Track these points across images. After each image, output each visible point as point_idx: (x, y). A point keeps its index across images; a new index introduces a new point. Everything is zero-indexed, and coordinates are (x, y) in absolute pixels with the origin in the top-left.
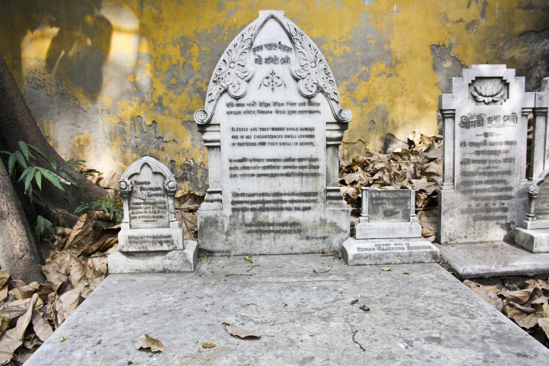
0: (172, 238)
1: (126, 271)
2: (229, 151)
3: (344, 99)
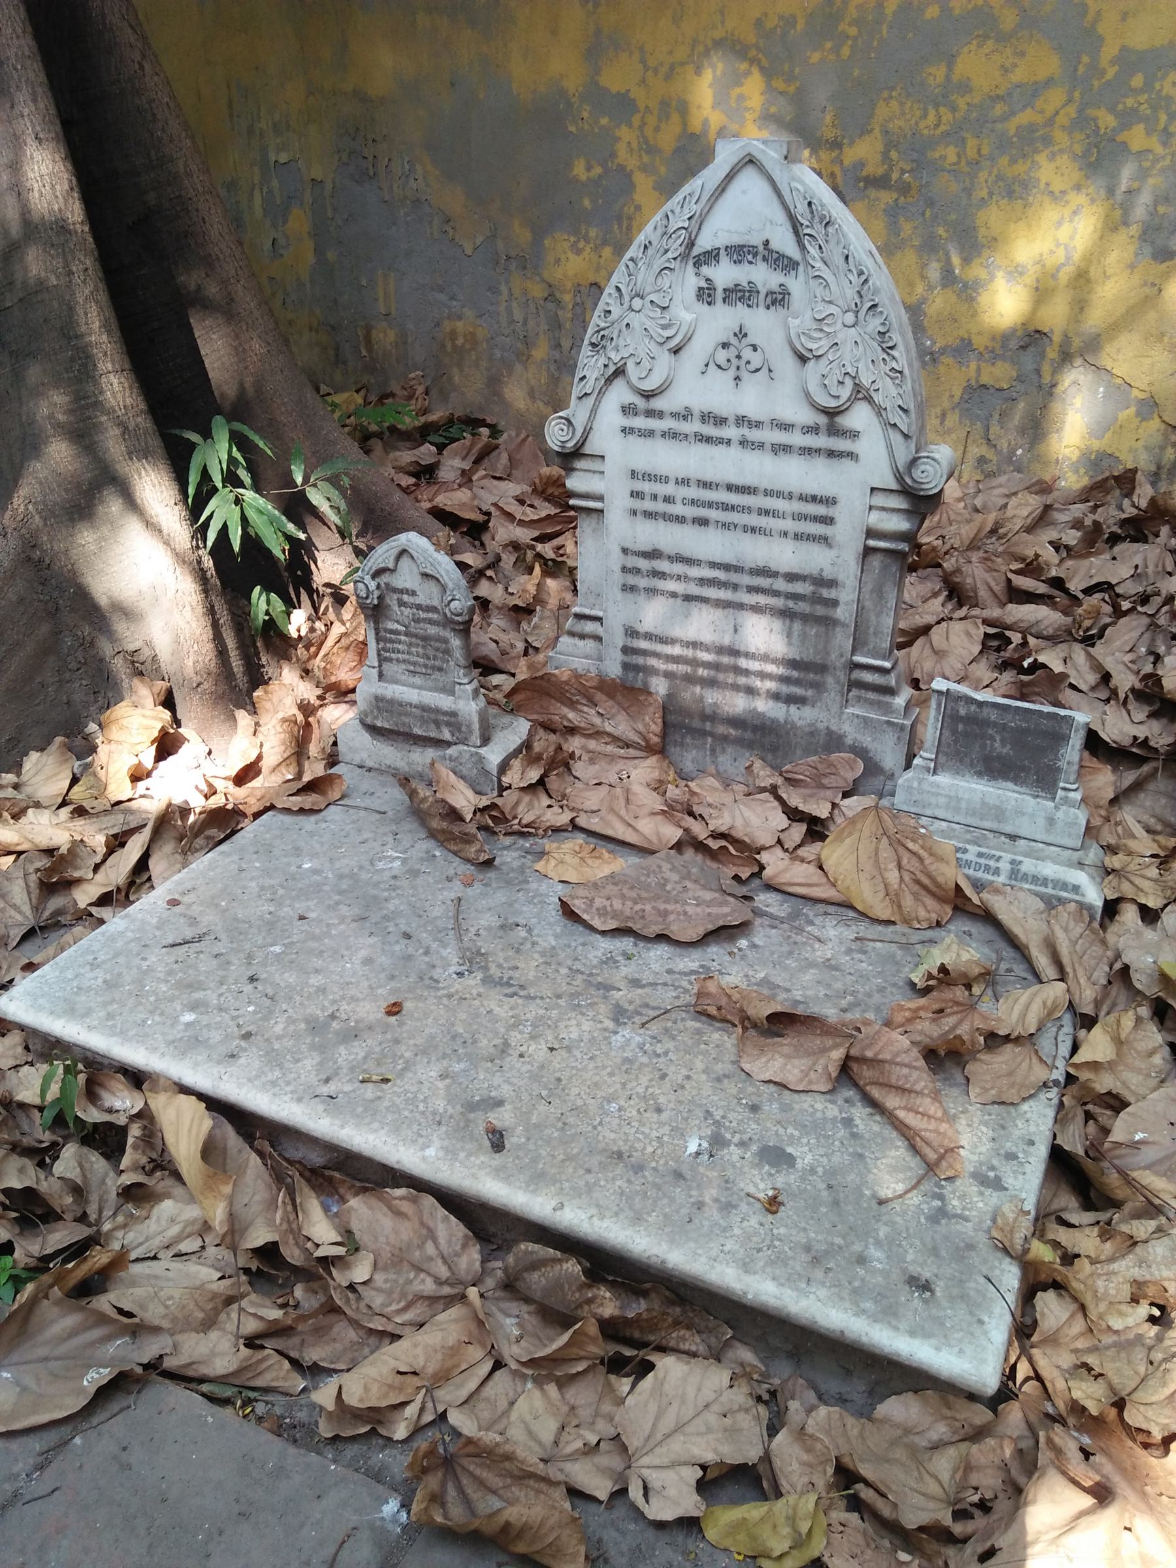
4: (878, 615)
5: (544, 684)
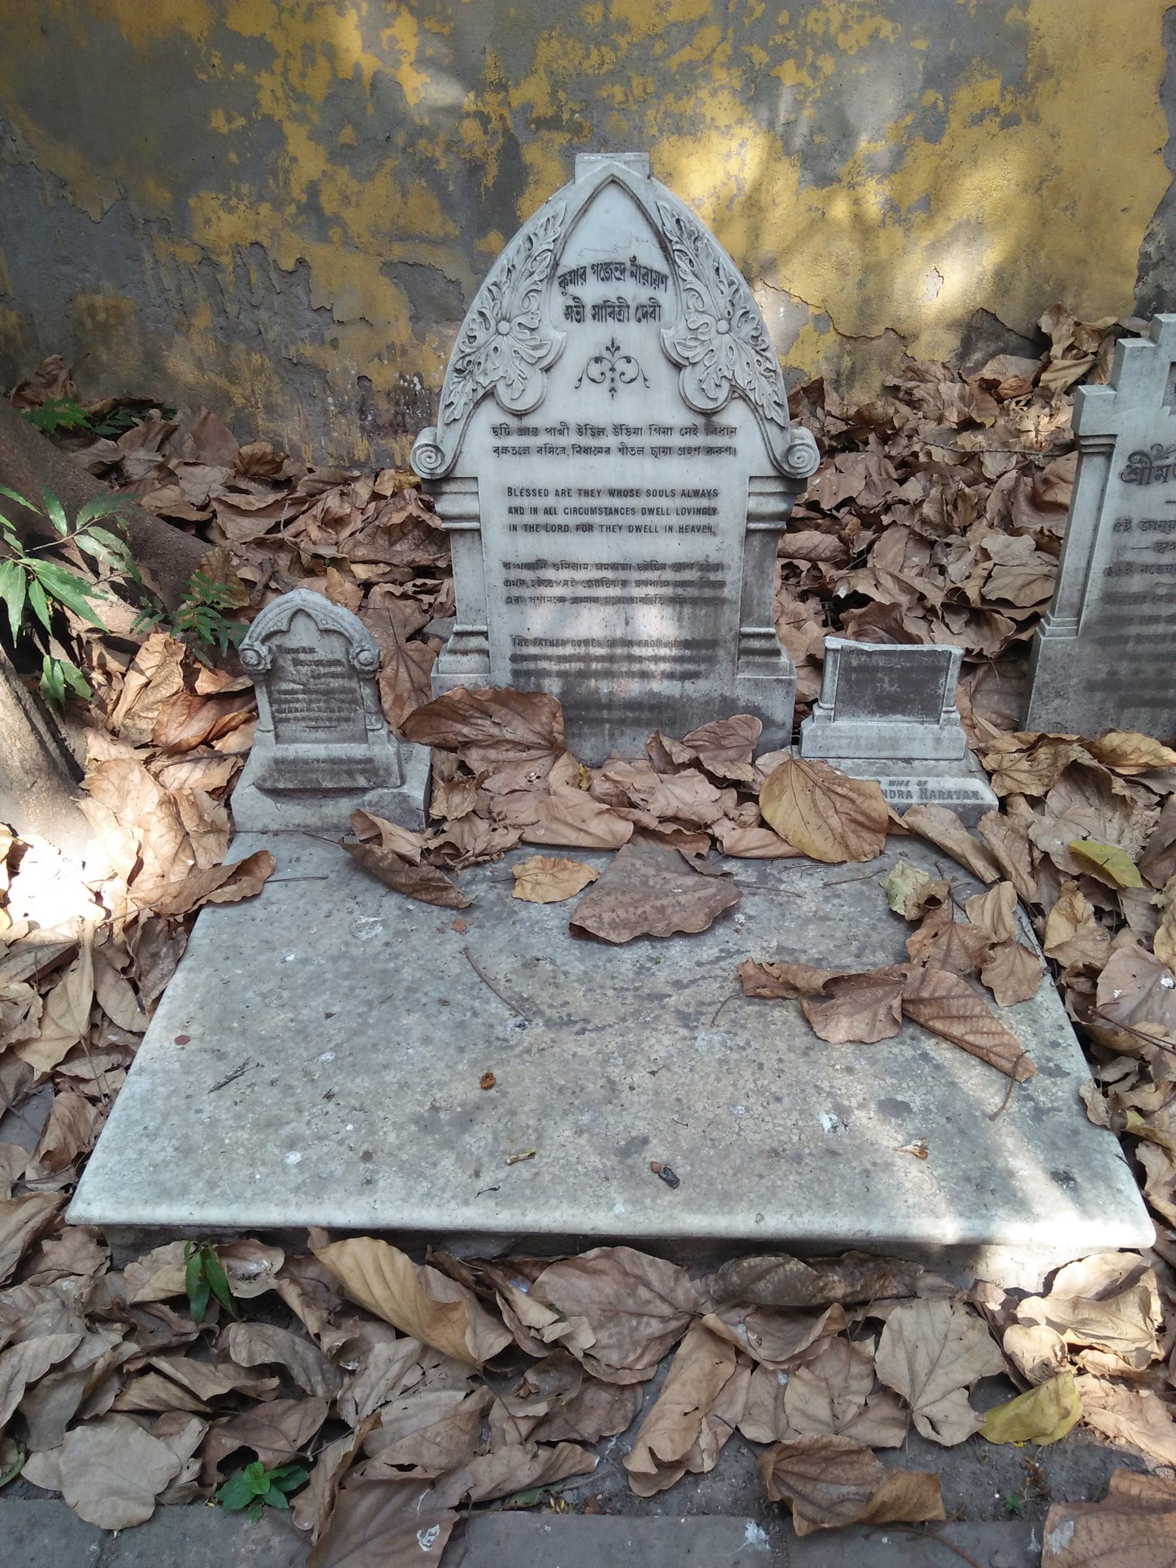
2: (501, 543)
4: (760, 588)
5: (437, 707)
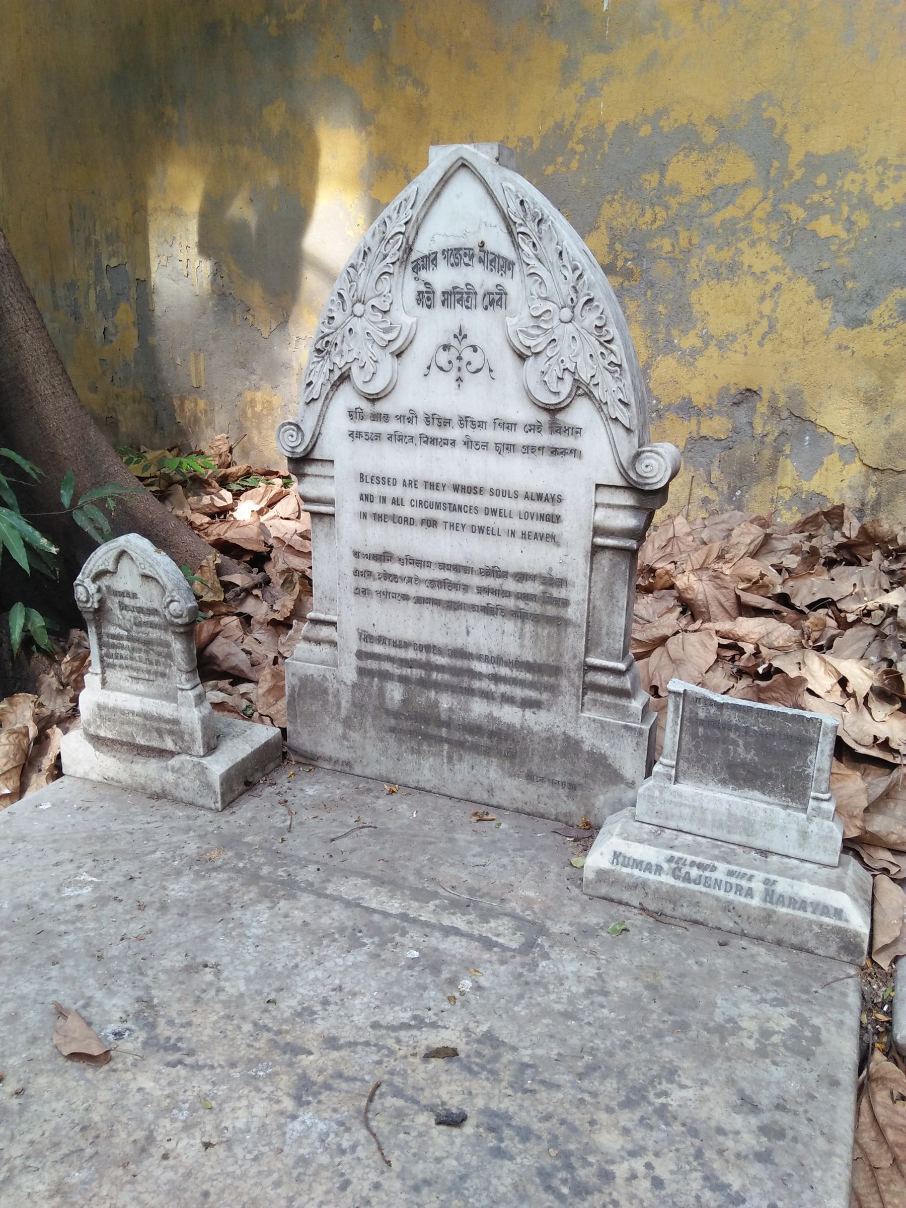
0: (182, 727)
1: (94, 776)
2: (352, 531)
3: (886, 343)
4: (609, 615)
